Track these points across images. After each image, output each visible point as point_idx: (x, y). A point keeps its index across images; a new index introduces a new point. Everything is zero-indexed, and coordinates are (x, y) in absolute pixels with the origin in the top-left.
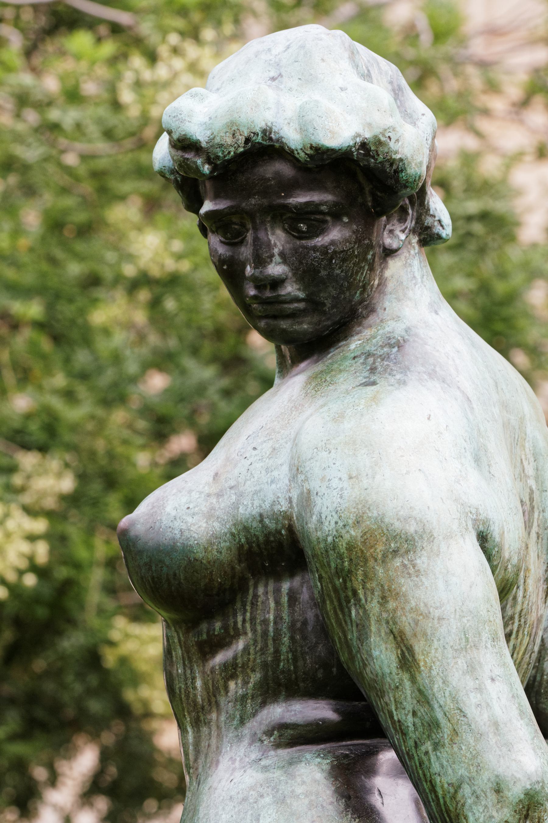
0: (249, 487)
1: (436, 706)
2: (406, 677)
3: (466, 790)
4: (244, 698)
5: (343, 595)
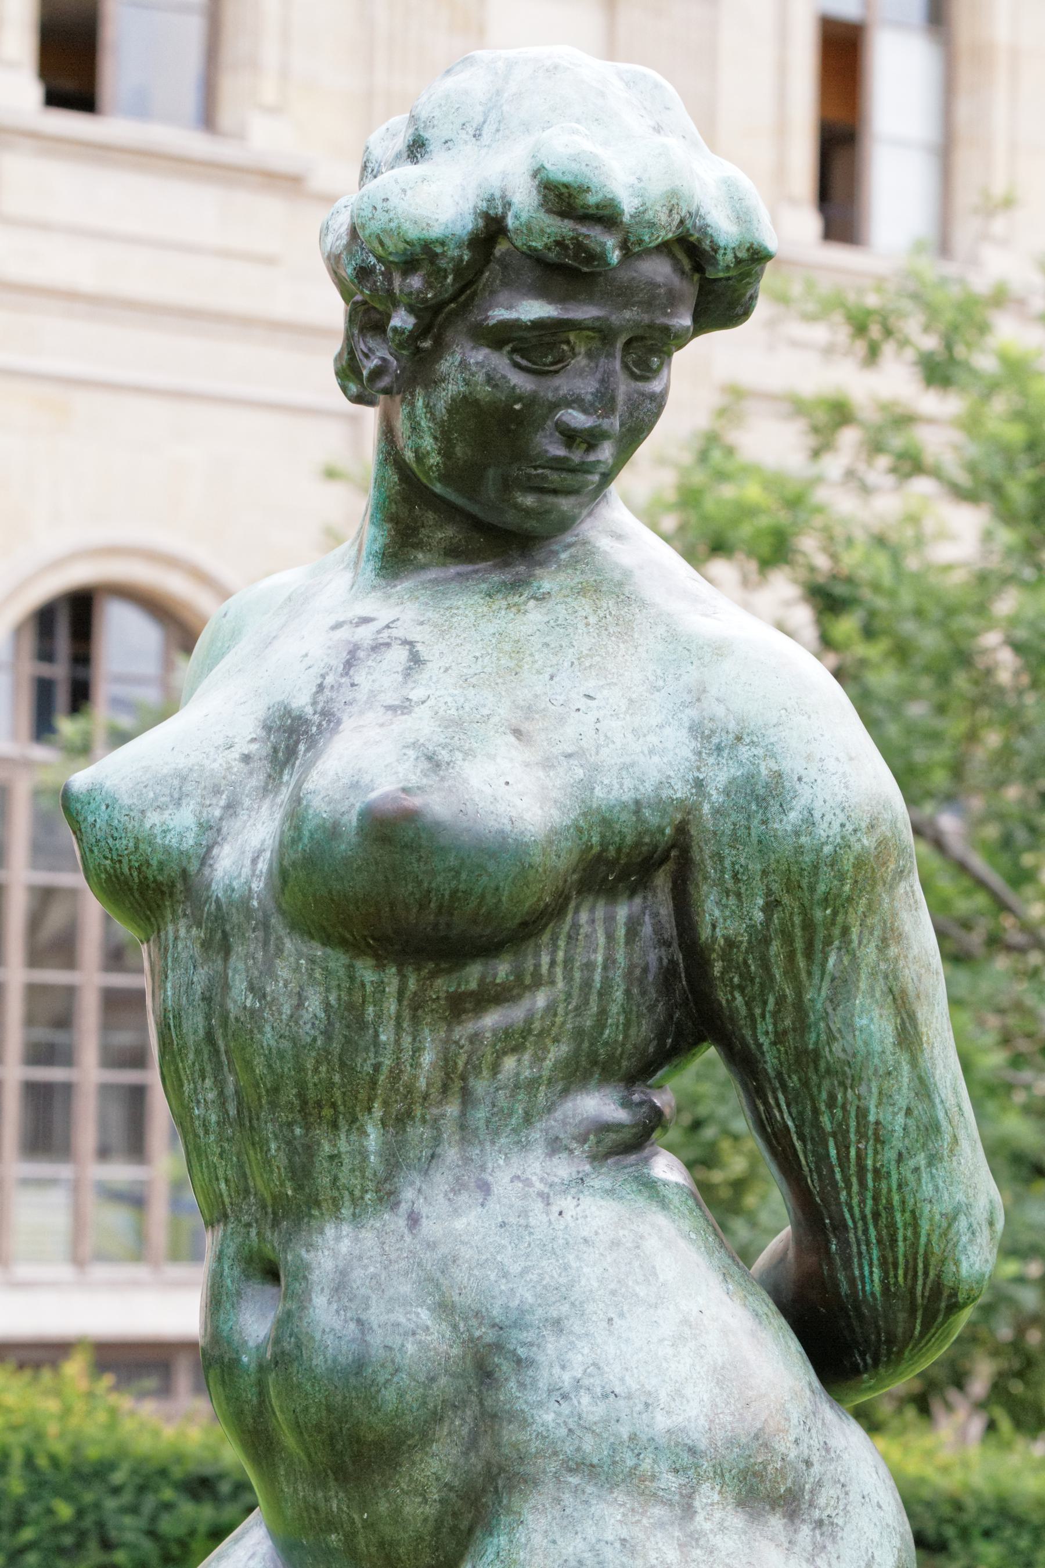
1: (937, 1101)
2: (904, 1058)
4: (533, 1084)
5: (821, 933)
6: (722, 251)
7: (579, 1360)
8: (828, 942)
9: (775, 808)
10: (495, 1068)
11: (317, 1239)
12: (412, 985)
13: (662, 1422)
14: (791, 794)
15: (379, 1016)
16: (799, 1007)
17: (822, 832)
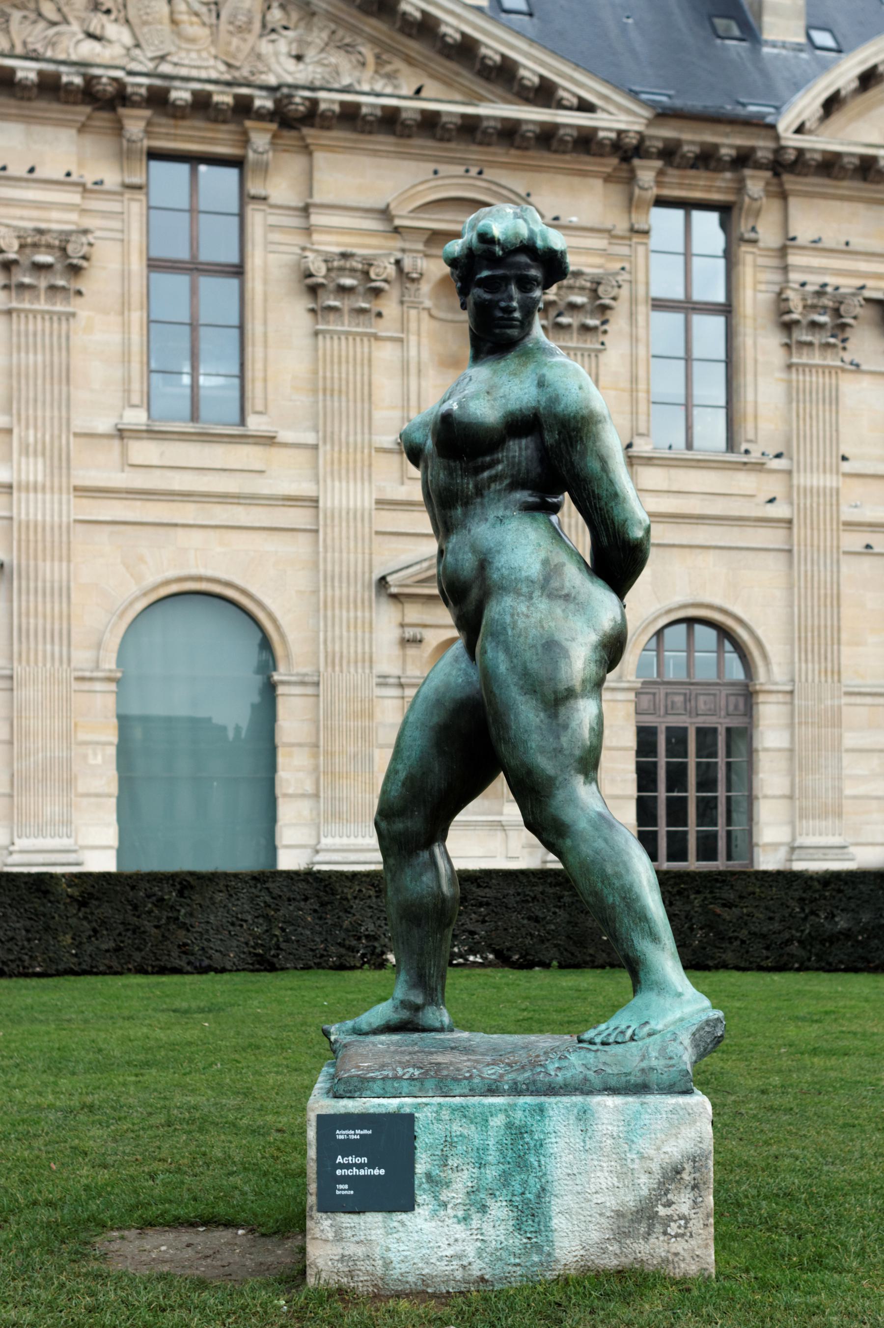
0: (513, 396)
3: (629, 522)
4: (500, 491)
7: (503, 560)
10: (489, 487)
11: (612, 624)
13: (524, 574)
16: (572, 463)
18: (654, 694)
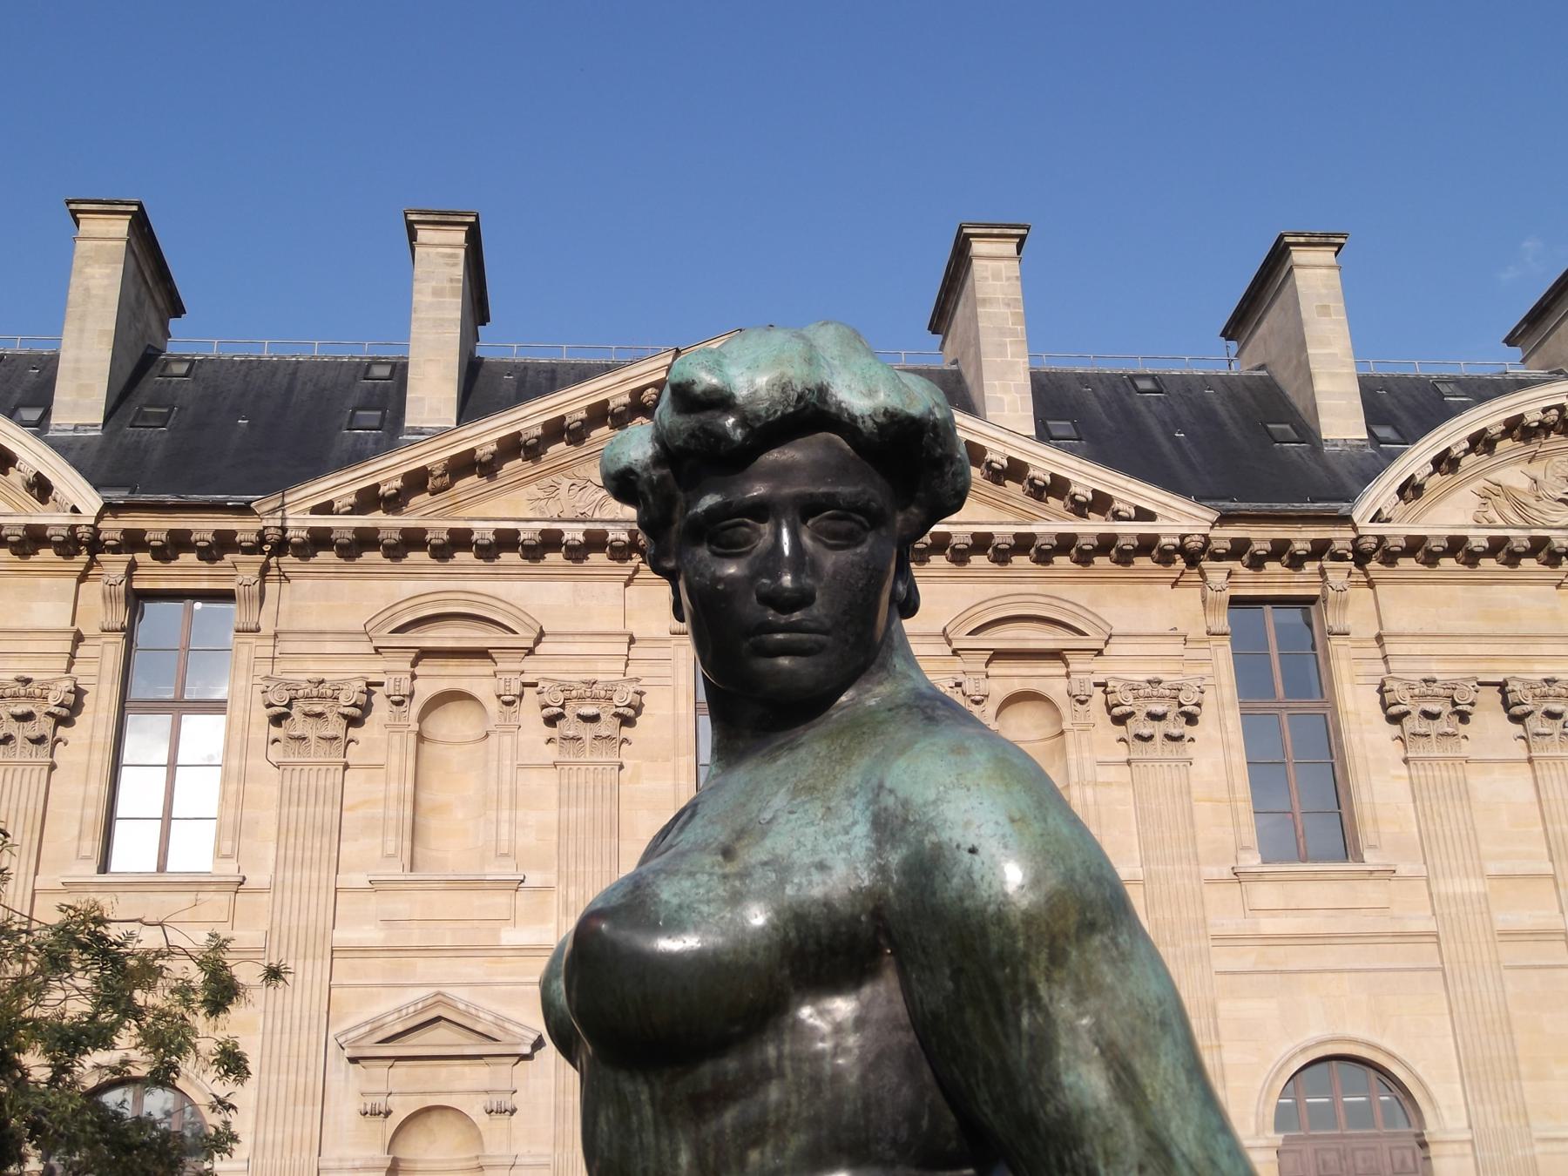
1: (1177, 1155)
2: (1125, 1114)
5: (1007, 994)
6: (860, 420)
8: (1017, 1001)
9: (939, 879)
10: (742, 1161)
12: (660, 1093)
14: (952, 862)
15: (641, 1124)
17: (983, 893)
18: (1300, 1152)
